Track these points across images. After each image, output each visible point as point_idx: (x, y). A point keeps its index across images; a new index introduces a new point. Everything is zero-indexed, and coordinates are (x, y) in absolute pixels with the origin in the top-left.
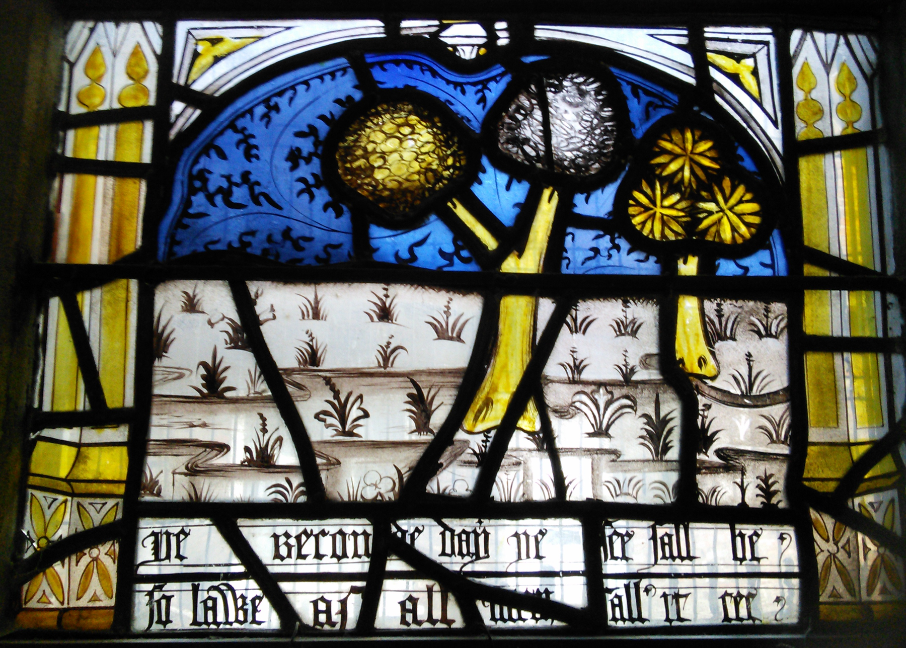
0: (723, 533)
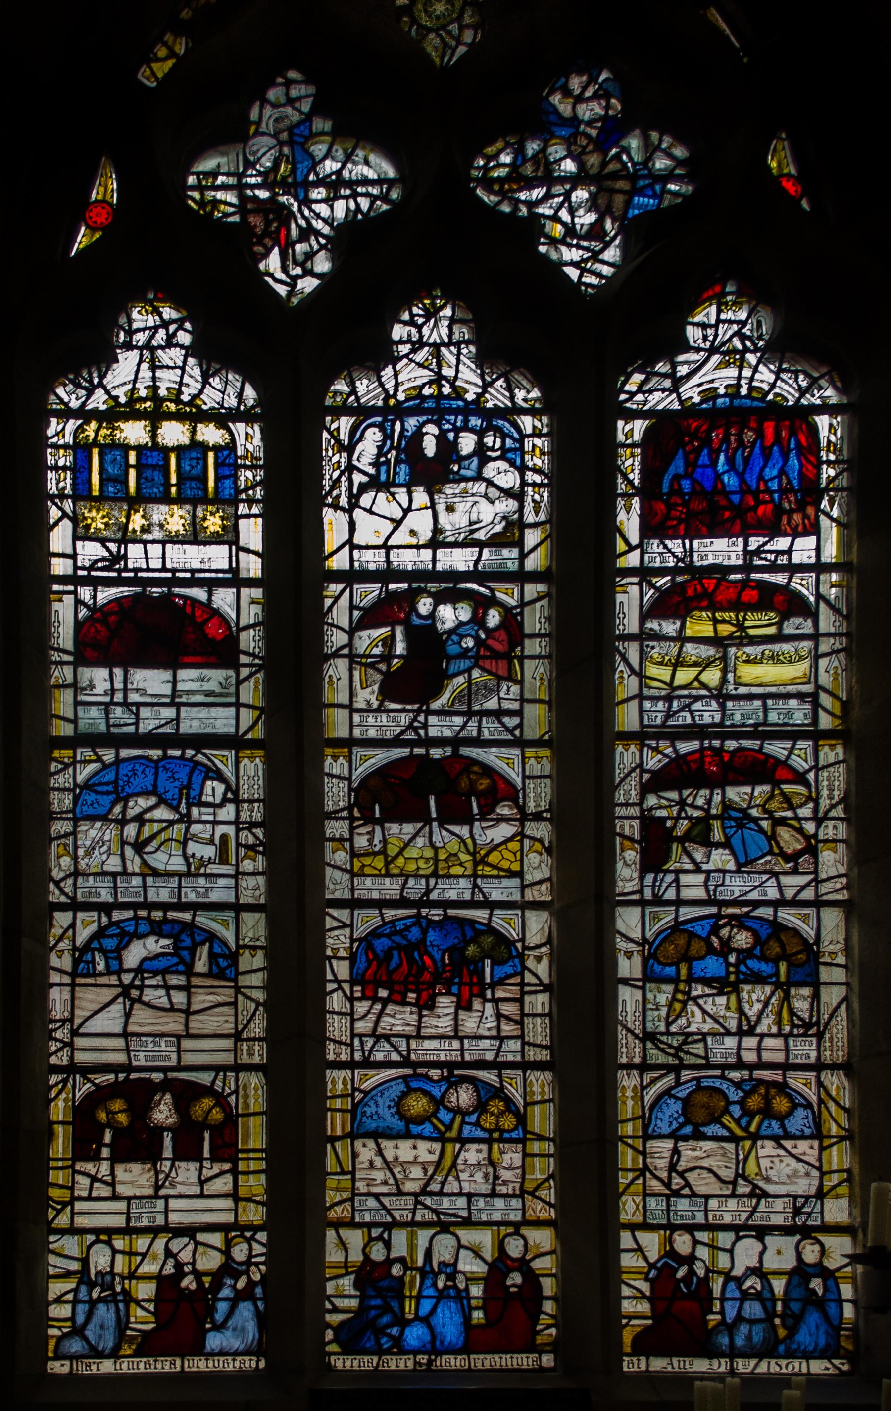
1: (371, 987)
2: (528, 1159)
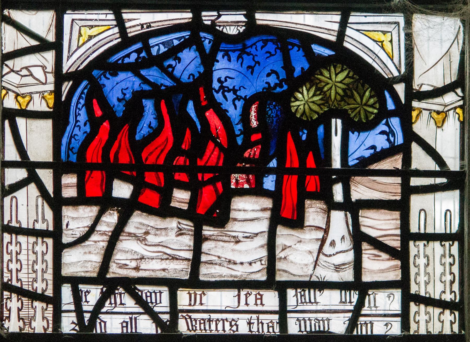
1: (97, 176)
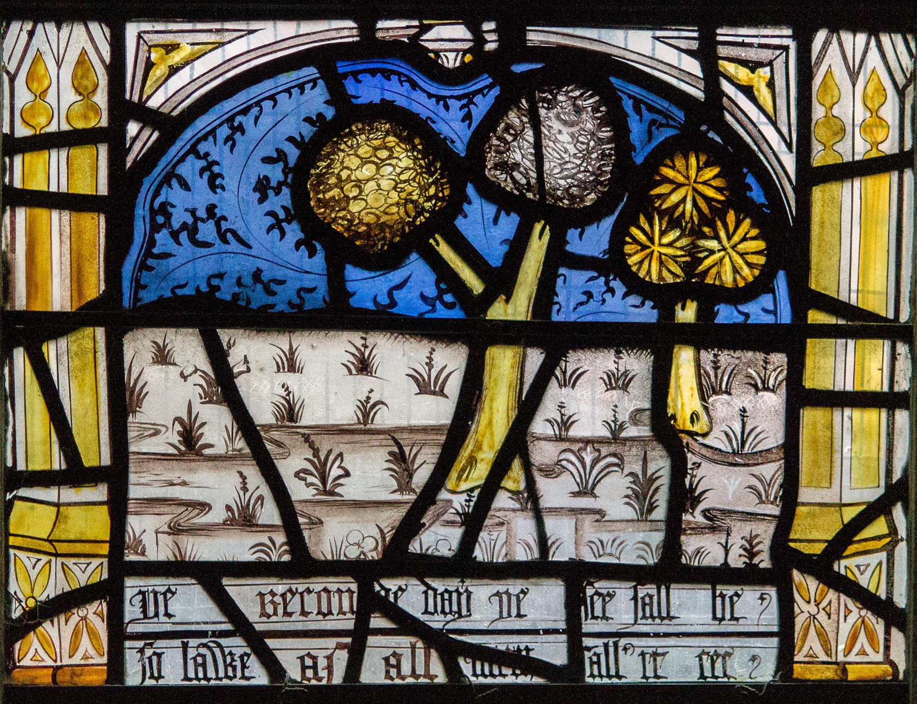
0: (701, 595)
2: (810, 417)
